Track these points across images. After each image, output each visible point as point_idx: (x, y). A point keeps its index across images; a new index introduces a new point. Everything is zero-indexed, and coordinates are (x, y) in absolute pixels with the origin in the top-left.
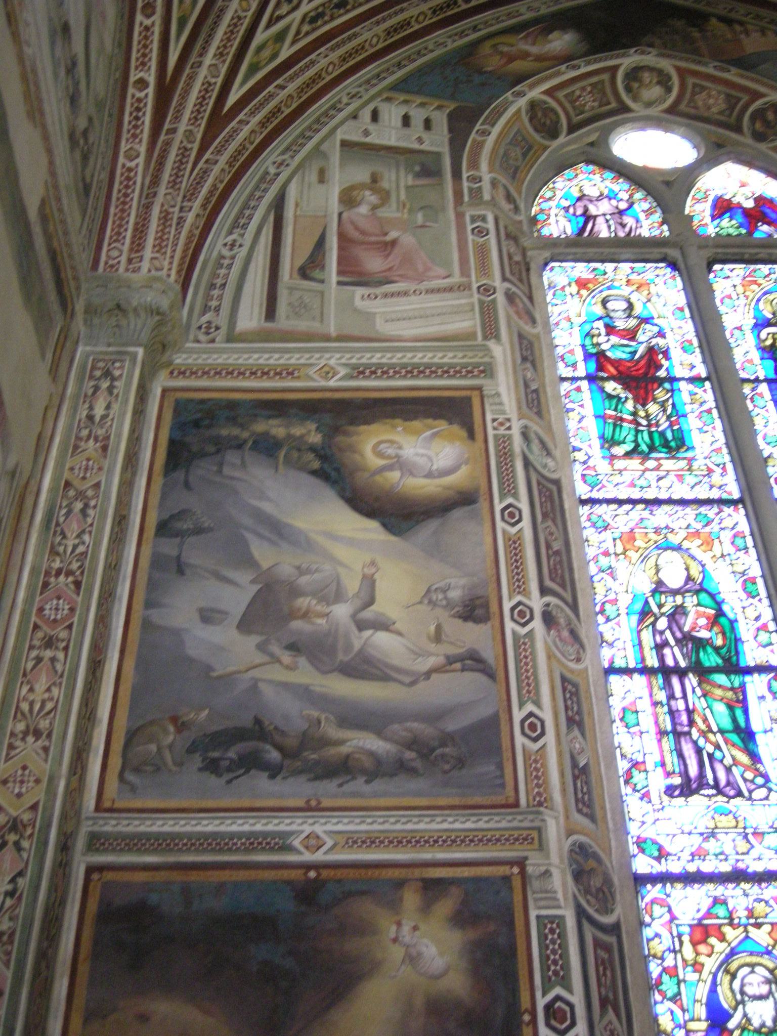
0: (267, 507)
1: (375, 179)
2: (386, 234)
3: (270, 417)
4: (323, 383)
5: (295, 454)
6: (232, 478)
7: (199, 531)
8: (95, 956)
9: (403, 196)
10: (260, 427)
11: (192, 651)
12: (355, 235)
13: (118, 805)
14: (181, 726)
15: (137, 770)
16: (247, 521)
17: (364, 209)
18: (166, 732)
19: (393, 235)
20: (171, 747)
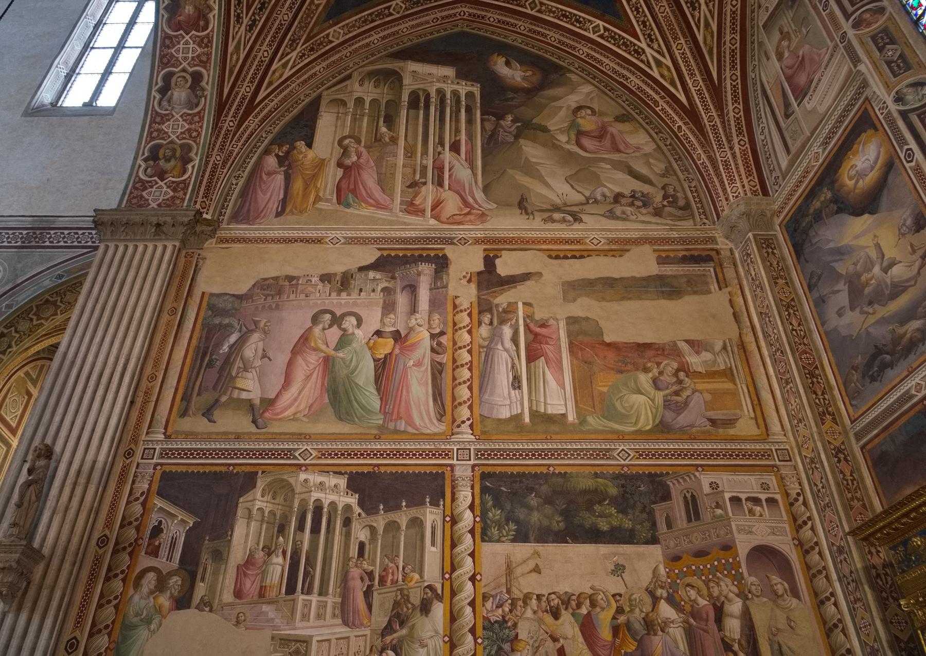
0: (832, 245)
1: (781, 33)
2: (799, 56)
3: (812, 201)
4: (818, 164)
5: (827, 210)
6: (816, 243)
7: (819, 277)
8: (880, 483)
9: (793, 27)
10: (812, 210)
11: (844, 332)
12: (790, 72)
13: (856, 417)
14: (855, 368)
15: (854, 398)
16: (829, 258)
17: (786, 54)
18: (853, 375)
19: (801, 53)
20: (857, 380)
